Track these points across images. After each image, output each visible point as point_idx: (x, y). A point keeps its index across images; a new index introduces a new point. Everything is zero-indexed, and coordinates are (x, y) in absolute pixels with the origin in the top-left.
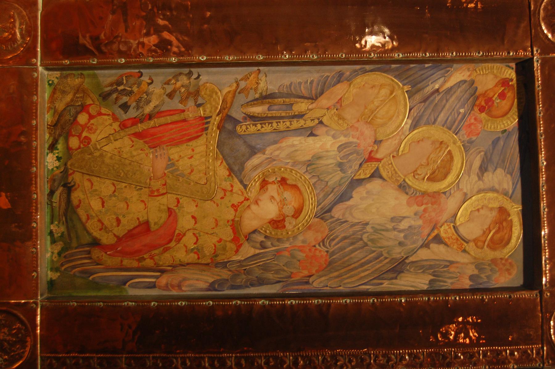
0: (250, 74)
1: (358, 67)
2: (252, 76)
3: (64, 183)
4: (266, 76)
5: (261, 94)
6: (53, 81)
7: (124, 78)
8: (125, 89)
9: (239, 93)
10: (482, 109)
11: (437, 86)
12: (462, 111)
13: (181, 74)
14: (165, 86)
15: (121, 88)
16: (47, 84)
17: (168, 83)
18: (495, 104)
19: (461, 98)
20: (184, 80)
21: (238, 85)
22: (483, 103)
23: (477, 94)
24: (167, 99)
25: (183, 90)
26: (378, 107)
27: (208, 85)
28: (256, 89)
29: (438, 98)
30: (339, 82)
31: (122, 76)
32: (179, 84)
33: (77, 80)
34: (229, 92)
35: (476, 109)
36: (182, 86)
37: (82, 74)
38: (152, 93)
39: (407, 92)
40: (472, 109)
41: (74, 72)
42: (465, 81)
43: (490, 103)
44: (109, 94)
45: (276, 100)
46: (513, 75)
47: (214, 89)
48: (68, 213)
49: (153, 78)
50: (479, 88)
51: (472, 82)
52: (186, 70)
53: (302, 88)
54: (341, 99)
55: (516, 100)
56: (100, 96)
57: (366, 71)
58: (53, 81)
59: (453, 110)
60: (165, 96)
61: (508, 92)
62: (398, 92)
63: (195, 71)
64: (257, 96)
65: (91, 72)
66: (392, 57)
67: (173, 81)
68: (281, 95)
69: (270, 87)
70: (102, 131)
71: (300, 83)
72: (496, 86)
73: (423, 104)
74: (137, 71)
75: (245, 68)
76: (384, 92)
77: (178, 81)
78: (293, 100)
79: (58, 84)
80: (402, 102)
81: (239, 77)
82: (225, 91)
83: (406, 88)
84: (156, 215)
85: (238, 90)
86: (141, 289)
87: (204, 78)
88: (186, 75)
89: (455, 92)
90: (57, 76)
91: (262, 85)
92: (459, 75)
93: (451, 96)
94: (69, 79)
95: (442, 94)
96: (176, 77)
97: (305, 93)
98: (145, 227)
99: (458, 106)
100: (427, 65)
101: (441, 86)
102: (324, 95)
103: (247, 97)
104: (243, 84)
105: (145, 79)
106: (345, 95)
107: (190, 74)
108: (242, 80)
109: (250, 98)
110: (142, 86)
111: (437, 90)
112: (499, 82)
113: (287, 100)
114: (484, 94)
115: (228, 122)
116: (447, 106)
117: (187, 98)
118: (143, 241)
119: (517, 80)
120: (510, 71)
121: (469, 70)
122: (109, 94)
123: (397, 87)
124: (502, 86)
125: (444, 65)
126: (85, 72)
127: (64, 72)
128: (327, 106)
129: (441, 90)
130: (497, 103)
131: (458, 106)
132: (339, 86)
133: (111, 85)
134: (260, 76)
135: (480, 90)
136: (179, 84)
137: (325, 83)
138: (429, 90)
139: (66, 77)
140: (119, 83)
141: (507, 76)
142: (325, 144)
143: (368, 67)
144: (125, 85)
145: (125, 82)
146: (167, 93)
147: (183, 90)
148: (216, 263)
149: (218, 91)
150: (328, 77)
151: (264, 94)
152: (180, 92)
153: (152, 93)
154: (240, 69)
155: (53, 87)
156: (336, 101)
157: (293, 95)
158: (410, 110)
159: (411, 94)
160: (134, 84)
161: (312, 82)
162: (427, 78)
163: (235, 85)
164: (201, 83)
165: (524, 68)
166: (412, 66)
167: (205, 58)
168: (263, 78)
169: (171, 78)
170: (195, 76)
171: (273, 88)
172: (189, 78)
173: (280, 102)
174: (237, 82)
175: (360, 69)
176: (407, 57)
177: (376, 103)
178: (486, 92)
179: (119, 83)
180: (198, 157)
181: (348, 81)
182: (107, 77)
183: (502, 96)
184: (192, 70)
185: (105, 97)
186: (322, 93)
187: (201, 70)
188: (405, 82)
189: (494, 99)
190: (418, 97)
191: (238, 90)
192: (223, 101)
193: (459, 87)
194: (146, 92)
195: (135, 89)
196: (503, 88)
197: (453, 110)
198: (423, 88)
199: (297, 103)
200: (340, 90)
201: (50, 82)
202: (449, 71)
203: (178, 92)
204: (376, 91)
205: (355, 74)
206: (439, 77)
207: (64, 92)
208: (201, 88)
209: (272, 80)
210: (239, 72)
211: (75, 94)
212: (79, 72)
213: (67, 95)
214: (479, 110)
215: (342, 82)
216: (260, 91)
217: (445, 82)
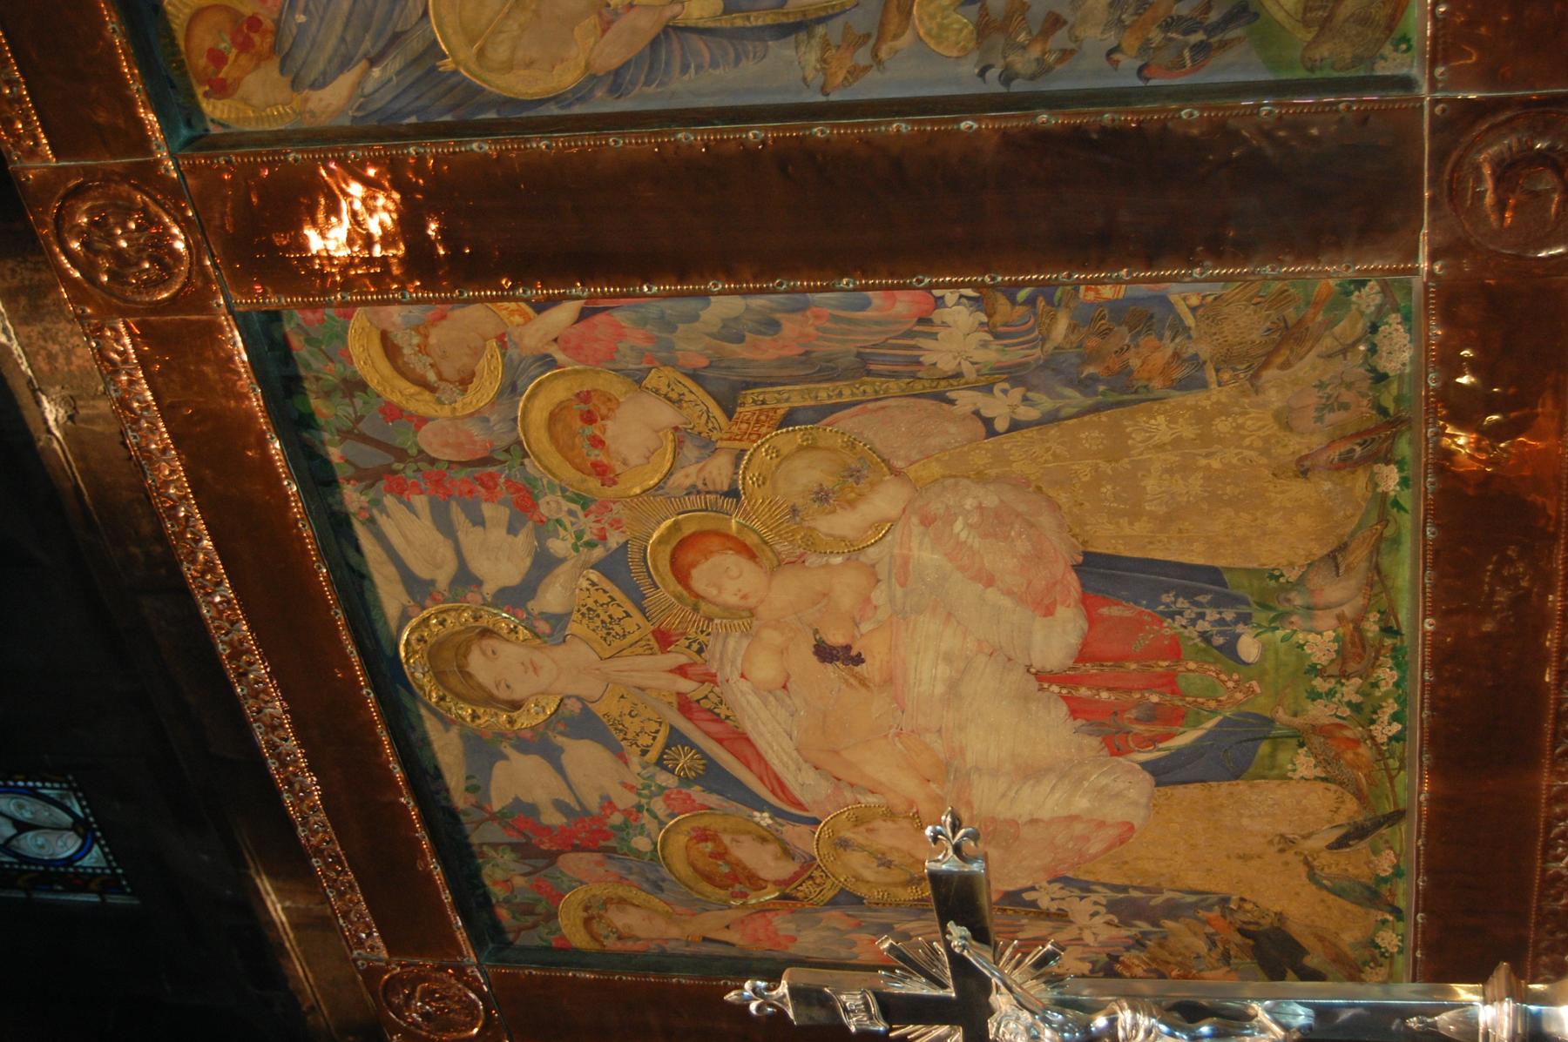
0: (846, 83)
1: (578, 110)
2: (840, 78)
4: (804, 79)
5: (811, 36)
6: (1396, 50)
7: (1188, 63)
8: (1187, 33)
9: (868, 36)
10: (254, 23)
11: (376, 72)
12: (301, 18)
13: (1033, 77)
14: (1071, 46)
15: (1199, 37)
16: (1414, 43)
17: (1065, 54)
18: (227, 38)
19: (312, 46)
20: (1022, 62)
21: (875, 55)
22: (256, 38)
23: (277, 60)
24: (1065, 12)
25: (1022, 37)
26: (507, 16)
27: (955, 54)
28: (826, 46)
29: (367, 45)
30: (617, 73)
31: (1197, 67)
32: (1035, 52)
33: (1326, 54)
34: (896, 37)
35: (268, 24)
36: (1024, 48)
37: (1312, 70)
38: (1107, 26)
39: (445, 57)
40: (277, 22)
41: (1335, 74)
42: (315, 86)
43: (240, 39)
44: (1228, 20)
45: (769, 21)
46: (207, 106)
47: (939, 44)
49: (1106, 65)
50: (276, 74)
51: (295, 84)
52: (1018, 86)
53: (707, 55)
54: (604, 31)
55: (182, 48)
56: (1256, 15)
57: (556, 99)
58: (1396, 50)
59: (322, 19)
60: (1071, 20)
61: (205, 68)
62: (467, 54)
63: (993, 85)
64: (820, 30)
65: (1285, 76)
66: (496, 142)
67: (1051, 58)
68: (759, 33)
69: (789, 53)
71: (714, 64)
72: (238, 81)
73: (399, 29)
74: (1152, 83)
75: (860, 97)
76: (500, 53)
77: (1037, 60)
78: (725, 23)
79: (1380, 43)
80: (450, 31)
81: (874, 75)
82: (906, 39)
83: (448, 65)
85: (872, 42)
87: (969, 68)
88: (1017, 76)
89: (330, 61)
90: (1382, 63)
91: (812, 58)
93: (336, 50)
94: (1348, 56)
95: (361, 52)
96: (1043, 69)
97: (697, 42)
99: (314, 27)
100: (413, 120)
101: (366, 74)
102: (647, 41)
103: (847, 27)
104: (862, 56)
105: (1129, 62)
106: (596, 42)
107: (1008, 77)
108: (867, 69)
109: (837, 24)
110: (1137, 44)
111: (373, 62)
112: (235, 91)
113: (739, 23)
114: (260, 60)
116: (338, 27)
117: (1008, 17)
119: (193, 96)
120: (217, 115)
121: (313, 114)
122: (1228, 20)
123: (474, 67)
124: (224, 80)
125: (373, 122)
126: (1301, 74)
127: (1362, 73)
128: (633, 13)
129: (364, 64)
130: (223, 40)
131: (314, 27)
132: (615, 62)
133: (1224, 45)
134: (820, 79)
135: (271, 69)
136: (1035, 52)
137: (651, 67)
138: (394, 63)
139: (1358, 60)
140: (1202, 50)
141: (219, 104)
143: (554, 110)
144: (1186, 44)
145: (1187, 53)
146: (1065, 29)
147: (1022, 37)
149: (927, 39)
150: (647, 83)
151: (802, 36)
152: (1030, 32)
153: (1107, 26)
154: (876, 94)
155: (1397, 34)
156: (614, 28)
158: (425, 13)
159: (432, 50)
160: (1158, 48)
161: (685, 68)
162: (404, 91)
163: (883, 54)
164: (975, 57)
166: (448, 118)
167: (963, 125)
168: (810, 74)
169: (1059, 67)
170: (993, 74)
171: (782, 51)
172: (1007, 67)
173: (757, 18)
174: (880, 63)
175: (570, 105)
176: (459, 144)
177: (513, 26)
178: (257, 66)
179: (1202, 50)
181: (594, 76)
182: (1237, 65)
183: (218, 58)
184: (1002, 89)
186: (655, 44)
187: (975, 88)
188: (454, 80)
189: (234, 51)
190: (415, 45)
191: (872, 42)
192: (910, 13)
193: (324, 73)
194: (1125, 28)
195: (1156, 36)
196: (221, 75)
197: (322, 19)
198: (408, 66)
199: (714, 18)
200: (611, 54)
201: (1404, 47)
202: (360, 108)
203: (1035, 33)
204: (520, 54)
205: (580, 94)
206: (377, 95)
207: (1364, 20)
208: (971, 45)
209: (788, 72)
210: (873, 88)
211: (1329, 18)
212: (1318, 75)
213: (1352, 15)
214: (259, 22)
215: (609, 73)
216: (815, 42)
217: (359, 84)
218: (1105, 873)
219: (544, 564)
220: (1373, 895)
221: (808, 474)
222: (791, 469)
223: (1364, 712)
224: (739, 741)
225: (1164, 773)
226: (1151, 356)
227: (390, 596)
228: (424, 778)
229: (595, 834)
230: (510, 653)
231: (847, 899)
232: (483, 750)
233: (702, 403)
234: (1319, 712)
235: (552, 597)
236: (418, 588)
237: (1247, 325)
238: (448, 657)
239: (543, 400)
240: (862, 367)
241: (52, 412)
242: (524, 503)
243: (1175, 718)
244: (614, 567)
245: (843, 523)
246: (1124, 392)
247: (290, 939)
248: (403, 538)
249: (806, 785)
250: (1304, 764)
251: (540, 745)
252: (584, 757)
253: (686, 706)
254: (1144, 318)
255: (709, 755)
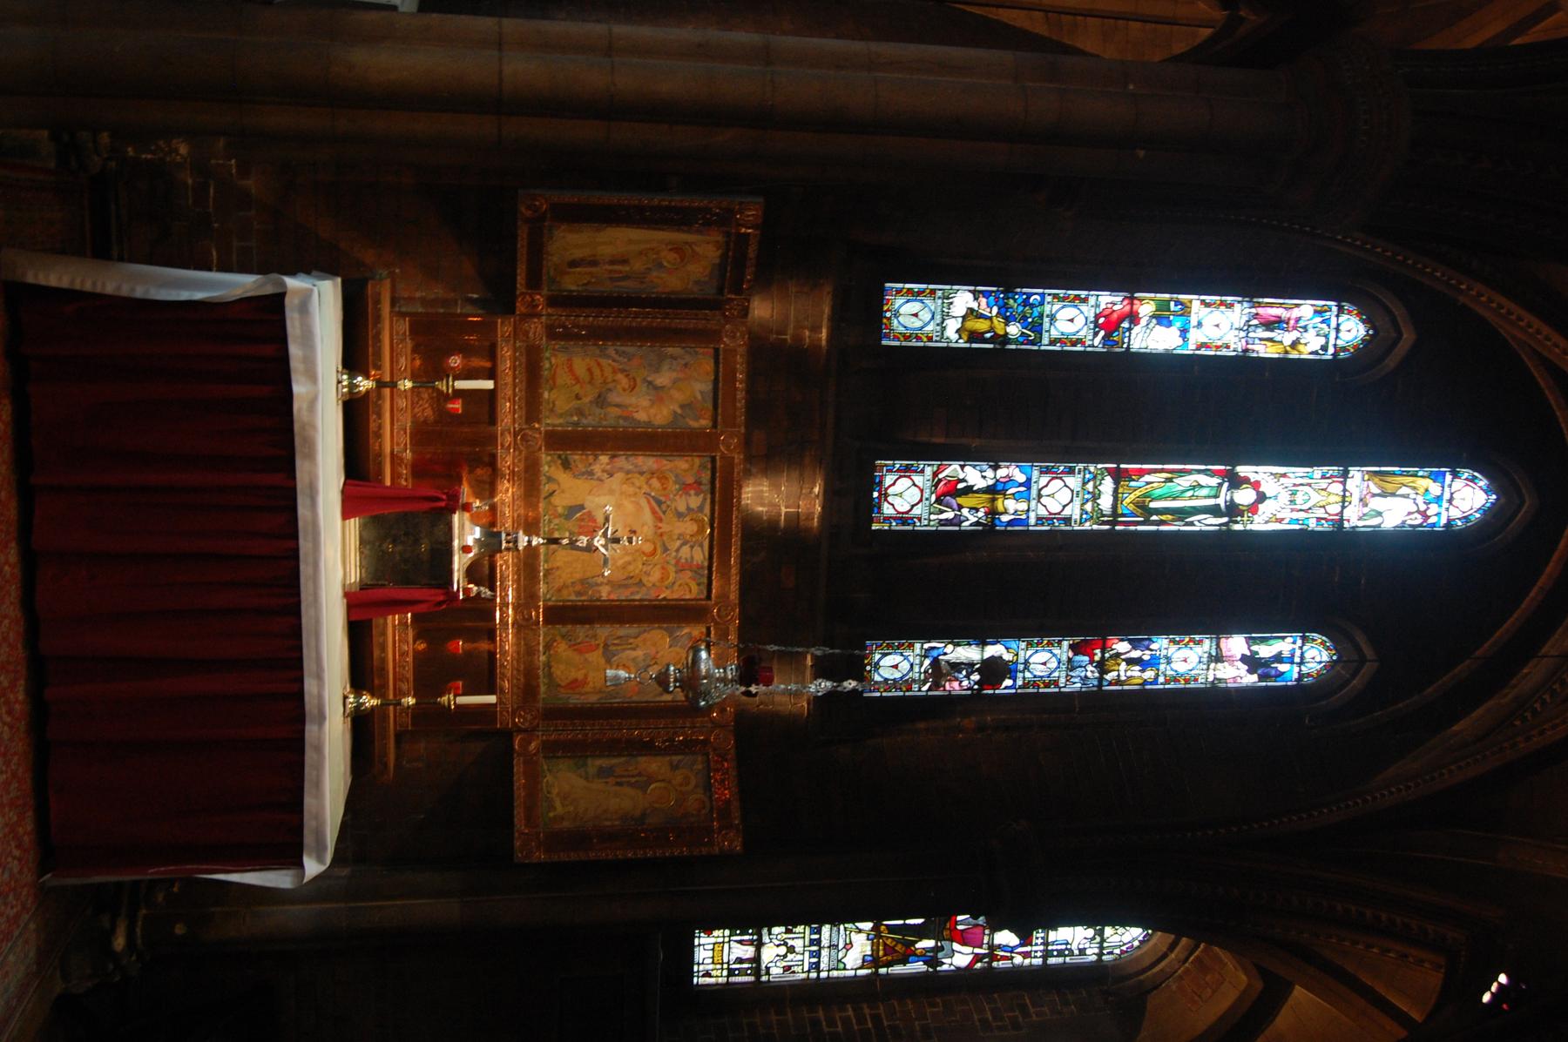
3: (548, 665)
48: (550, 675)
70: (562, 648)
84: (580, 675)
86: (575, 700)
92: (686, 630)
98: (575, 681)
115: (606, 646)
118: (574, 684)
142: (639, 653)
148: (600, 691)
157: (628, 637)
165: (708, 629)
180: (596, 657)
185: (563, 637)
218: (595, 483)
219: (677, 550)
220: (550, 479)
221: (631, 568)
222: (637, 568)
223: (550, 521)
224: (654, 512)
225: (582, 507)
226: (578, 588)
227: (706, 544)
228: (713, 502)
229: (685, 488)
230: (689, 532)
231: (642, 473)
232: (701, 509)
233: (645, 580)
234: (556, 521)
235: (678, 543)
236: (701, 546)
237: (565, 592)
238: (701, 530)
239: (671, 579)
240: (620, 586)
241: (816, 490)
242: (677, 562)
243: (581, 519)
244: (666, 549)
245: (627, 558)
246: (583, 581)
247: (825, 322)
248: (700, 556)
249: (644, 503)
250: (560, 510)
251: (689, 509)
252: (682, 508)
253: (661, 520)
254: (579, 594)
255: (659, 506)
